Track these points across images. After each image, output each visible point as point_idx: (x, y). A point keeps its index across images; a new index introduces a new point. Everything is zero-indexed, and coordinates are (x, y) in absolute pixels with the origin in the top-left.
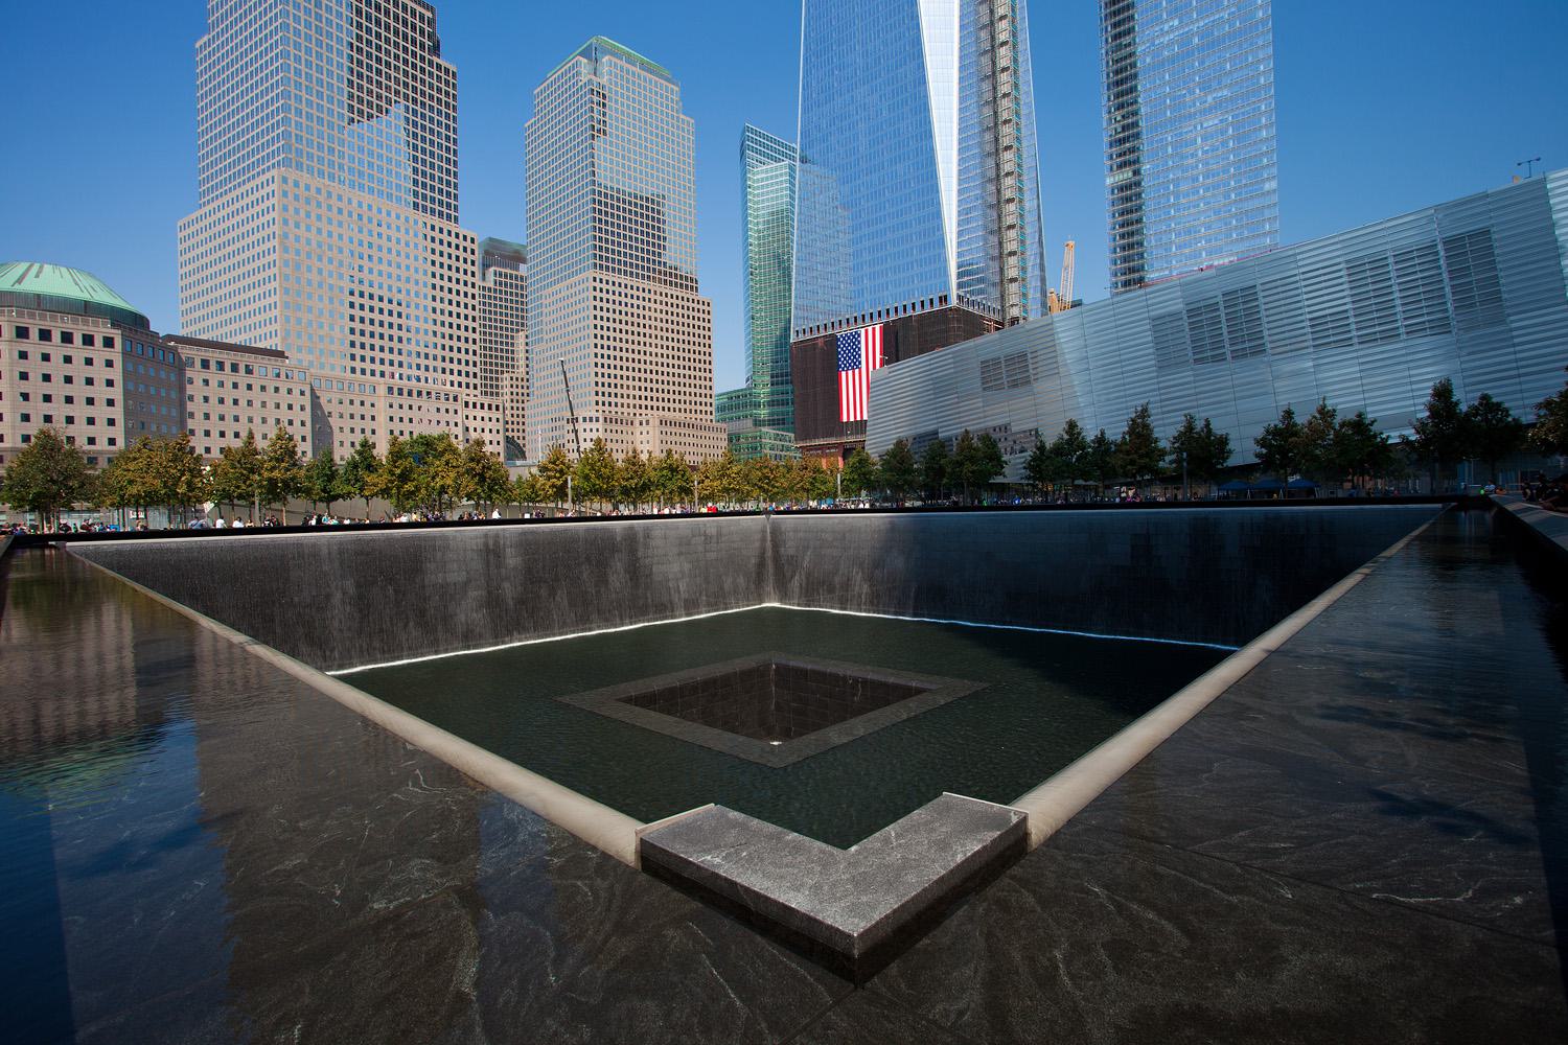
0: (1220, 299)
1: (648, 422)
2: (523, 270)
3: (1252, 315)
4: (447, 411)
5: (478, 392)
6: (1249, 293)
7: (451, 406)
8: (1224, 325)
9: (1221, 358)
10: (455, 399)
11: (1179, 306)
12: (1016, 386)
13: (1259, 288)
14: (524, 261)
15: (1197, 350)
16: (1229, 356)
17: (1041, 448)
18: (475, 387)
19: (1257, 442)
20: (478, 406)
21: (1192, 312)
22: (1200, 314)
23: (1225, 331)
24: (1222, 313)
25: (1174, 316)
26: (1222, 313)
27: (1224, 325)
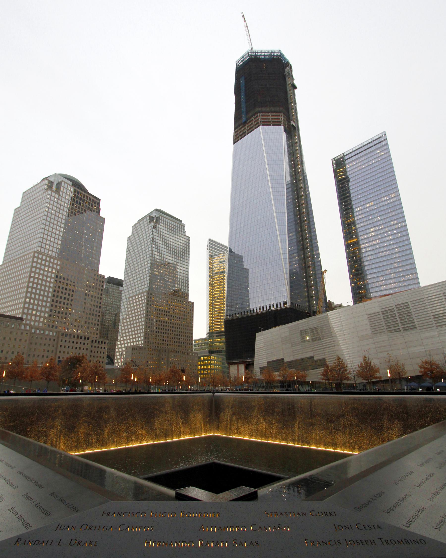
0: (394, 307)
1: (165, 351)
2: (121, 288)
3: (409, 314)
4: (84, 344)
5: (98, 336)
6: (406, 305)
7: (86, 341)
8: (397, 317)
9: (398, 331)
10: (88, 339)
11: (378, 310)
12: (315, 341)
13: (409, 303)
14: (122, 286)
15: (388, 327)
16: (401, 329)
17: (328, 367)
18: (97, 334)
19: (419, 366)
20: (97, 342)
21: (384, 312)
22: (387, 314)
23: (398, 319)
24: (396, 312)
25: (377, 313)
26: (396, 312)
27: (397, 317)
